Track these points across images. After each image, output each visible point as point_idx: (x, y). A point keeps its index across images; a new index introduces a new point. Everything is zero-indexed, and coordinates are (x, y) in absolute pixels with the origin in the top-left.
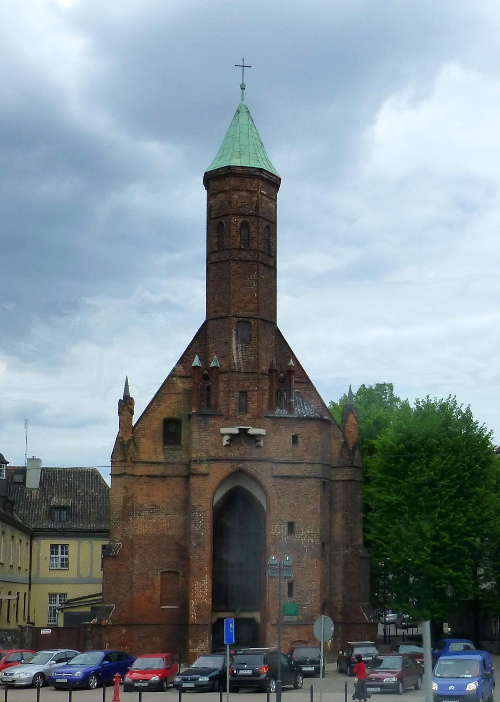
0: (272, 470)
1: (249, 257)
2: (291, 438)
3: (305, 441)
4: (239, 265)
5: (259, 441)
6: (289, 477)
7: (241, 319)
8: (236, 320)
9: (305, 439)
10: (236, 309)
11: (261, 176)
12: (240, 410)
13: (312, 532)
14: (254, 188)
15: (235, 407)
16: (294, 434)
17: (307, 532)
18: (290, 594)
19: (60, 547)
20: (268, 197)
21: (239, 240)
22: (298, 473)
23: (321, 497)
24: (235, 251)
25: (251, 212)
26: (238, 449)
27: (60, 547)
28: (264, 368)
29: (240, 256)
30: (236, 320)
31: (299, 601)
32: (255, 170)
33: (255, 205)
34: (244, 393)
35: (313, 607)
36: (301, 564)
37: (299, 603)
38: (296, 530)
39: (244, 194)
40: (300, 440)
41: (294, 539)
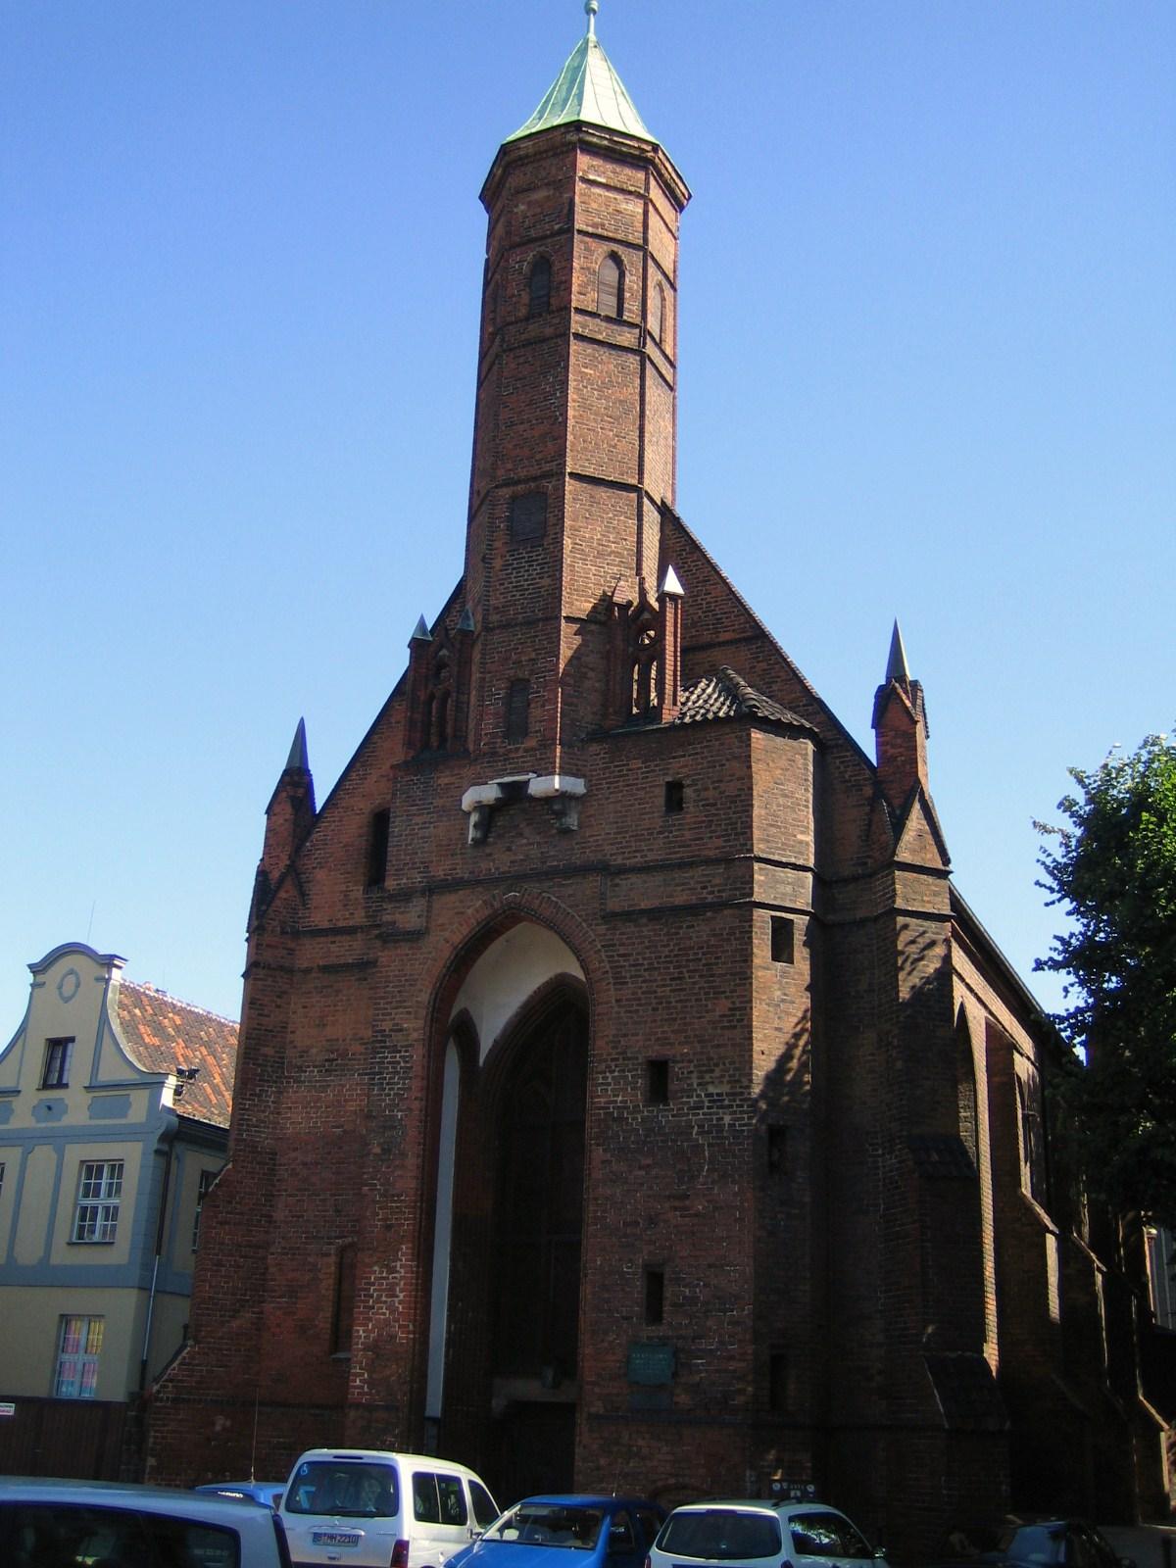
3: (704, 794)
4: (521, 360)
5: (561, 814)
6: (654, 914)
10: (509, 466)
12: (507, 735)
13: (725, 1088)
16: (669, 779)
17: (711, 1089)
21: (525, 298)
22: (681, 898)
25: (557, 227)
26: (509, 849)
30: (506, 492)
32: (563, 130)
33: (565, 211)
35: (731, 1358)
36: (687, 1203)
38: (673, 1086)
39: (540, 195)
40: (688, 792)
41: (666, 1116)
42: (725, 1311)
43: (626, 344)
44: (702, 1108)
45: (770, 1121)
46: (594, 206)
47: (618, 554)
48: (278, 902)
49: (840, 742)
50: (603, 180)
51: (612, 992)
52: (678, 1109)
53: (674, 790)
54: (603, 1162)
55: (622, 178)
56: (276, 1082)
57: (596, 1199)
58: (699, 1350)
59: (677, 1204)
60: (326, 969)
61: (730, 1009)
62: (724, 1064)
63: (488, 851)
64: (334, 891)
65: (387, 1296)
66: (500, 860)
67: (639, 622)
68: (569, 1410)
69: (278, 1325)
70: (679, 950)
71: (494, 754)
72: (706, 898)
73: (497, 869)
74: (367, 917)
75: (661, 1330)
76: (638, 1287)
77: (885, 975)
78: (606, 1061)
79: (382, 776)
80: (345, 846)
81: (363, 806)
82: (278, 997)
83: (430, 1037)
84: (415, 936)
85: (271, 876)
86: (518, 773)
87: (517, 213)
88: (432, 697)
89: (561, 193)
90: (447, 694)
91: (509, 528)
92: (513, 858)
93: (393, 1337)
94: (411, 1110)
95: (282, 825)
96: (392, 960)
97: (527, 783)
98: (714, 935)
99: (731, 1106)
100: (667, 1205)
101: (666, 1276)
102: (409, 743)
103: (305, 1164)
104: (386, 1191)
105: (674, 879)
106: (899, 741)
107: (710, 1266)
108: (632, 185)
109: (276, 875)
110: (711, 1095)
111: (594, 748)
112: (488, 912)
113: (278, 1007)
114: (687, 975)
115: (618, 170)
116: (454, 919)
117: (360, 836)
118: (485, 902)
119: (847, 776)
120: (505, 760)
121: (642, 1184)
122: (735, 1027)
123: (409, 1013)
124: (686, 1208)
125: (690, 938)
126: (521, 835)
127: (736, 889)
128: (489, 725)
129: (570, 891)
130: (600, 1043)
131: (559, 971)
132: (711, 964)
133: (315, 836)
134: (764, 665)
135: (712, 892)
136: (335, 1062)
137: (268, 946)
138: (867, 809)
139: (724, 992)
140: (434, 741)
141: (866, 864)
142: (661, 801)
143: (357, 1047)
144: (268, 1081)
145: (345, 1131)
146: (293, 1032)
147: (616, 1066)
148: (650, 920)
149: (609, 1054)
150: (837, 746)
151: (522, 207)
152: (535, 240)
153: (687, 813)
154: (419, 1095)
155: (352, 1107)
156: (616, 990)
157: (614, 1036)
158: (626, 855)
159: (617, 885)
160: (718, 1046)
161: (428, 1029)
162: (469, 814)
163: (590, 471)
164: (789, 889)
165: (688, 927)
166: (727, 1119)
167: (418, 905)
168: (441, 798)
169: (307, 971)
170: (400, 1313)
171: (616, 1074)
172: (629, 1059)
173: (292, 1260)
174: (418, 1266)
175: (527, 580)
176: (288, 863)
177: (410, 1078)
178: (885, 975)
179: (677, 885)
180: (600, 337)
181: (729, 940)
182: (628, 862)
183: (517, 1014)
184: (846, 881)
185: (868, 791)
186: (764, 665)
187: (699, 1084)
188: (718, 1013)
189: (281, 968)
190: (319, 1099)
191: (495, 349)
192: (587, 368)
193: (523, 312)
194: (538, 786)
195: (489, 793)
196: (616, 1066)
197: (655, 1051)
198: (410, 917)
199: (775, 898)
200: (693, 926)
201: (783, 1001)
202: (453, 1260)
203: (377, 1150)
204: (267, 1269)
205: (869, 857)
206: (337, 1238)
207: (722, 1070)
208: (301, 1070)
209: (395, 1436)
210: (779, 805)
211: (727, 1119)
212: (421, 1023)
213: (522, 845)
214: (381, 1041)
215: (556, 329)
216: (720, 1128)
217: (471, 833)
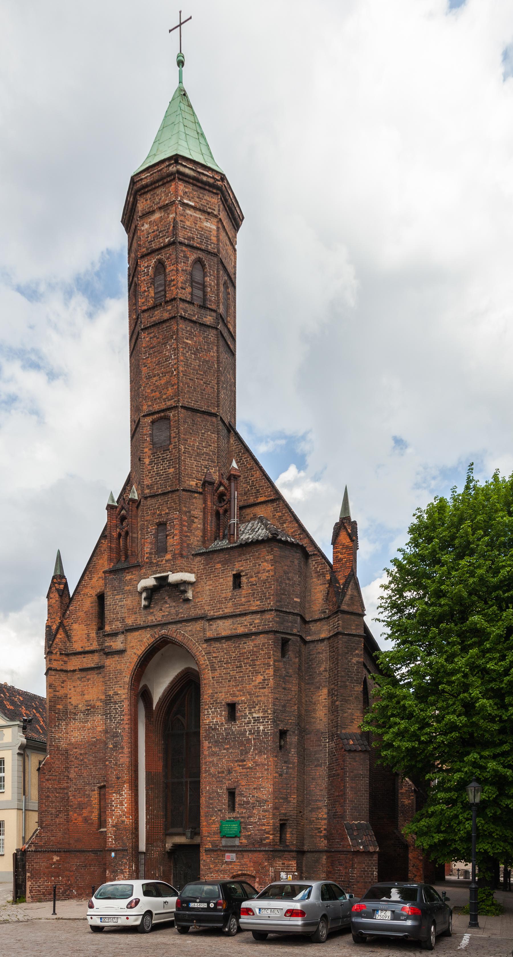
0: (204, 630)
1: (166, 316)
4: (152, 335)
5: (185, 592)
6: (228, 638)
7: (155, 416)
8: (149, 420)
9: (252, 577)
10: (150, 403)
11: (178, 172)
13: (261, 715)
15: (151, 549)
16: (235, 572)
17: (255, 715)
20: (200, 210)
22: (241, 630)
23: (275, 661)
24: (146, 315)
25: (167, 240)
28: (193, 483)
29: (154, 318)
30: (149, 420)
31: (242, 817)
33: (171, 228)
34: (162, 525)
35: (264, 825)
36: (245, 763)
37: (242, 820)
38: (238, 714)
39: (157, 216)
40: (244, 580)
41: (235, 728)
42: (261, 806)
43: (208, 323)
44: (250, 723)
45: (280, 728)
46: (188, 223)
47: (207, 454)
48: (57, 640)
49: (315, 553)
51: (210, 674)
52: (240, 724)
54: (208, 747)
55: (204, 202)
56: (65, 720)
57: (206, 763)
58: (251, 822)
59: (240, 764)
60: (82, 670)
61: (263, 680)
62: (260, 704)
63: (151, 611)
64: (82, 634)
65: (120, 805)
66: (157, 615)
67: (218, 492)
68: (196, 848)
69: (76, 820)
70: (240, 654)
71: (151, 563)
72: (252, 630)
73: (156, 619)
74: (98, 645)
75: (235, 815)
76: (225, 798)
77: (333, 663)
78: (208, 704)
79: (100, 578)
80: (85, 612)
81: (92, 592)
82: (62, 683)
83: (131, 697)
84: (121, 652)
85: (52, 628)
86: (163, 572)
87: (143, 231)
88: (120, 535)
89: (168, 214)
90: (127, 533)
91: (152, 440)
92: (163, 614)
93: (123, 822)
94: (125, 729)
95: (54, 603)
96: (110, 662)
97: (167, 577)
98: (256, 647)
99: (263, 722)
100: (236, 764)
101: (236, 793)
102: (110, 560)
103: (81, 754)
104: (116, 763)
105: (237, 621)
106: (344, 551)
107: (254, 789)
108: (209, 208)
109: (54, 627)
110: (255, 717)
111: (198, 558)
112: (152, 640)
113: (63, 687)
114: (243, 665)
115: (201, 196)
116: (137, 644)
117: (92, 607)
118: (151, 635)
119: (318, 569)
120: (157, 566)
121: (225, 756)
122: (265, 688)
123: (121, 687)
124: (245, 765)
125: (245, 648)
126: (166, 602)
127: (266, 625)
128: (147, 549)
129: (190, 628)
130: (205, 697)
131: (186, 666)
132: (254, 660)
133: (71, 608)
134: (280, 514)
135: (255, 627)
136: (90, 710)
137: (54, 660)
138: (327, 585)
139: (260, 672)
140: (123, 559)
141: (325, 612)
142: (231, 583)
143: (99, 704)
144: (61, 720)
145: (97, 740)
146: (70, 698)
147: (213, 706)
148: (226, 641)
149: (210, 701)
150: (314, 555)
151: (146, 226)
152: (153, 251)
153: (243, 589)
154: (127, 722)
155: (99, 729)
156: (212, 673)
157: (212, 693)
158: (215, 611)
159: (211, 625)
160: (258, 696)
161: (129, 693)
162: (140, 593)
163: (192, 405)
164: (290, 624)
165: (244, 643)
166: (262, 728)
167: (121, 638)
168: (128, 586)
169: (74, 671)
170: (125, 812)
171: (213, 710)
172: (219, 703)
173: (79, 793)
174: (132, 793)
175: (162, 470)
176: (60, 621)
177: (123, 715)
178: (333, 663)
179: (239, 624)
180: (194, 319)
181: (262, 648)
182: (216, 614)
183: (168, 687)
184: (316, 621)
185: (328, 577)
186: (280, 514)
187: (249, 713)
188: (257, 682)
189: (62, 670)
190: (85, 726)
191: (138, 328)
192: (187, 339)
193: (151, 303)
194: (173, 577)
195: (150, 582)
196: (213, 706)
197: (230, 700)
198: (117, 644)
199: (284, 629)
200: (246, 643)
201: (286, 676)
202: (146, 790)
203: (111, 746)
204: (69, 798)
205: (327, 609)
206: (97, 783)
207: (259, 707)
208: (75, 714)
209: (127, 860)
210: (286, 584)
211: (262, 728)
212: (126, 691)
213: (167, 608)
214: (109, 700)
215: (169, 314)
216: (258, 732)
217: (144, 603)
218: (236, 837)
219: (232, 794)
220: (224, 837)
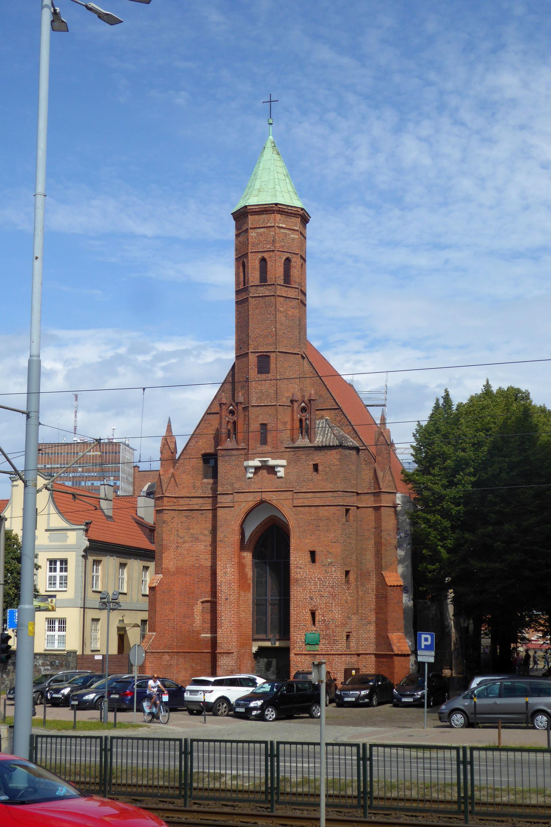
2: (312, 466)
14: (271, 223)
18: (314, 624)
19: (58, 563)
27: (58, 563)
40: (320, 468)
50: (284, 226)
53: (316, 468)
76: (309, 617)
89: (270, 232)
218: (317, 644)
219: (313, 614)
220: (308, 644)
